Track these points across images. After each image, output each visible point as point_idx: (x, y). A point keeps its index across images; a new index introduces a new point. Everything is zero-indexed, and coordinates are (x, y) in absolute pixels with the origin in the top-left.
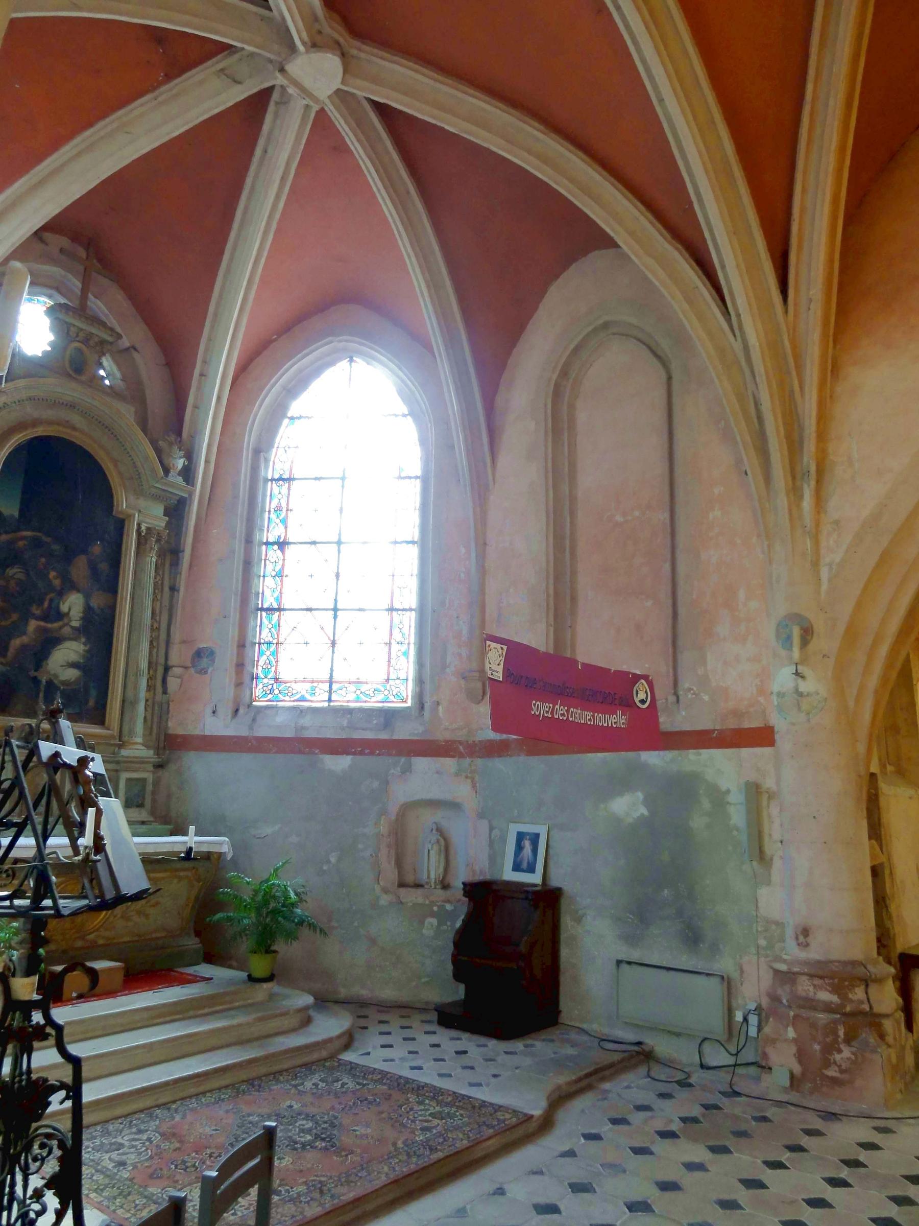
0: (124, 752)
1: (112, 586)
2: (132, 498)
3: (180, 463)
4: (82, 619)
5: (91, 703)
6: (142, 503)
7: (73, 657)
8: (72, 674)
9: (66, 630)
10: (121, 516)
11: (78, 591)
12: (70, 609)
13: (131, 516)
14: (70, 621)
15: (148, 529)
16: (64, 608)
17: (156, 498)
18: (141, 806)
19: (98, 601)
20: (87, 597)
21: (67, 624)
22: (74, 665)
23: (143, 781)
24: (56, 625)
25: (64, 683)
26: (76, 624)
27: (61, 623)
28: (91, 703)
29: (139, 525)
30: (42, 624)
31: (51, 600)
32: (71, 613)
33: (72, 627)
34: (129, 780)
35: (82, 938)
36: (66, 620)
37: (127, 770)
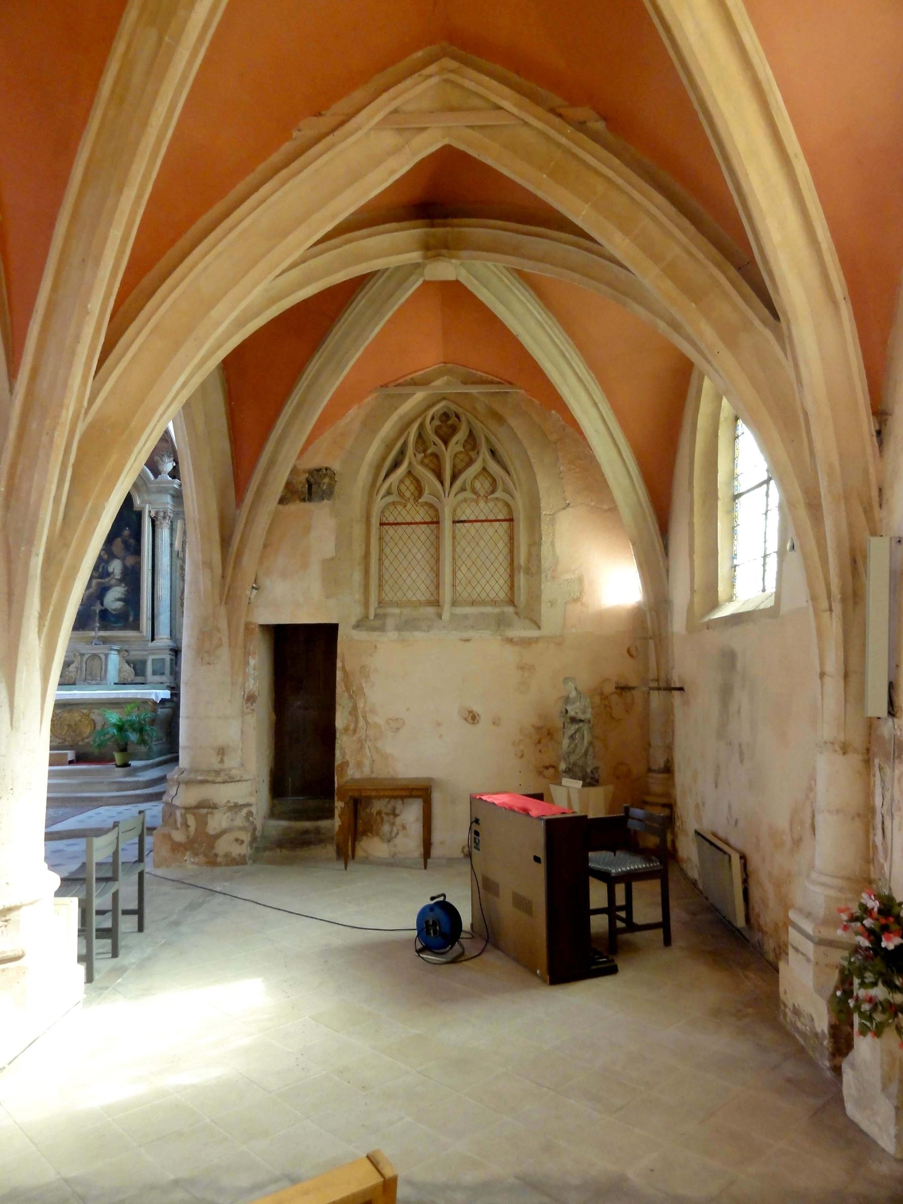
0: (151, 644)
1: (137, 551)
2: (146, 497)
3: (169, 466)
4: (121, 573)
5: (131, 619)
6: (153, 497)
7: (119, 595)
8: (119, 605)
9: (113, 582)
10: (139, 509)
11: (118, 558)
12: (114, 570)
13: (144, 508)
14: (114, 576)
15: (157, 513)
16: (110, 569)
17: (161, 491)
18: (163, 674)
19: (130, 561)
20: (123, 560)
21: (112, 579)
22: (119, 600)
23: (163, 660)
24: (107, 580)
25: (115, 610)
26: (118, 577)
27: (109, 578)
28: (131, 619)
29: (150, 512)
30: (100, 580)
31: (103, 567)
32: (115, 571)
33: (116, 579)
34: (153, 660)
35: (83, 740)
36: (112, 576)
37: (153, 654)
